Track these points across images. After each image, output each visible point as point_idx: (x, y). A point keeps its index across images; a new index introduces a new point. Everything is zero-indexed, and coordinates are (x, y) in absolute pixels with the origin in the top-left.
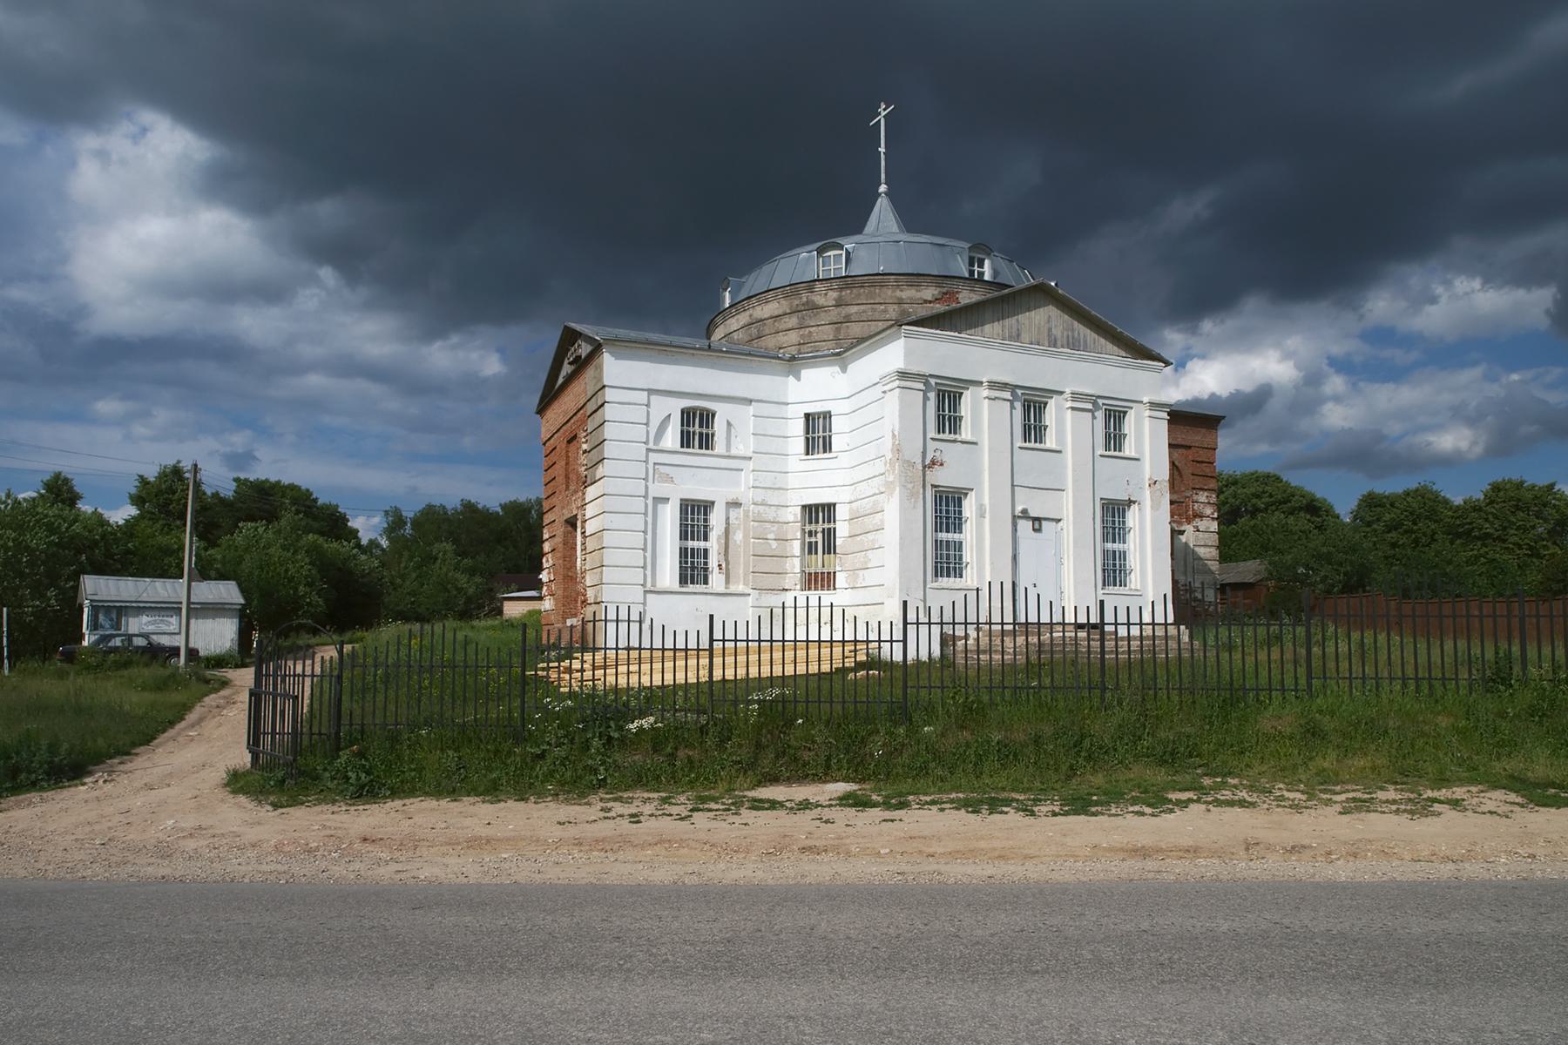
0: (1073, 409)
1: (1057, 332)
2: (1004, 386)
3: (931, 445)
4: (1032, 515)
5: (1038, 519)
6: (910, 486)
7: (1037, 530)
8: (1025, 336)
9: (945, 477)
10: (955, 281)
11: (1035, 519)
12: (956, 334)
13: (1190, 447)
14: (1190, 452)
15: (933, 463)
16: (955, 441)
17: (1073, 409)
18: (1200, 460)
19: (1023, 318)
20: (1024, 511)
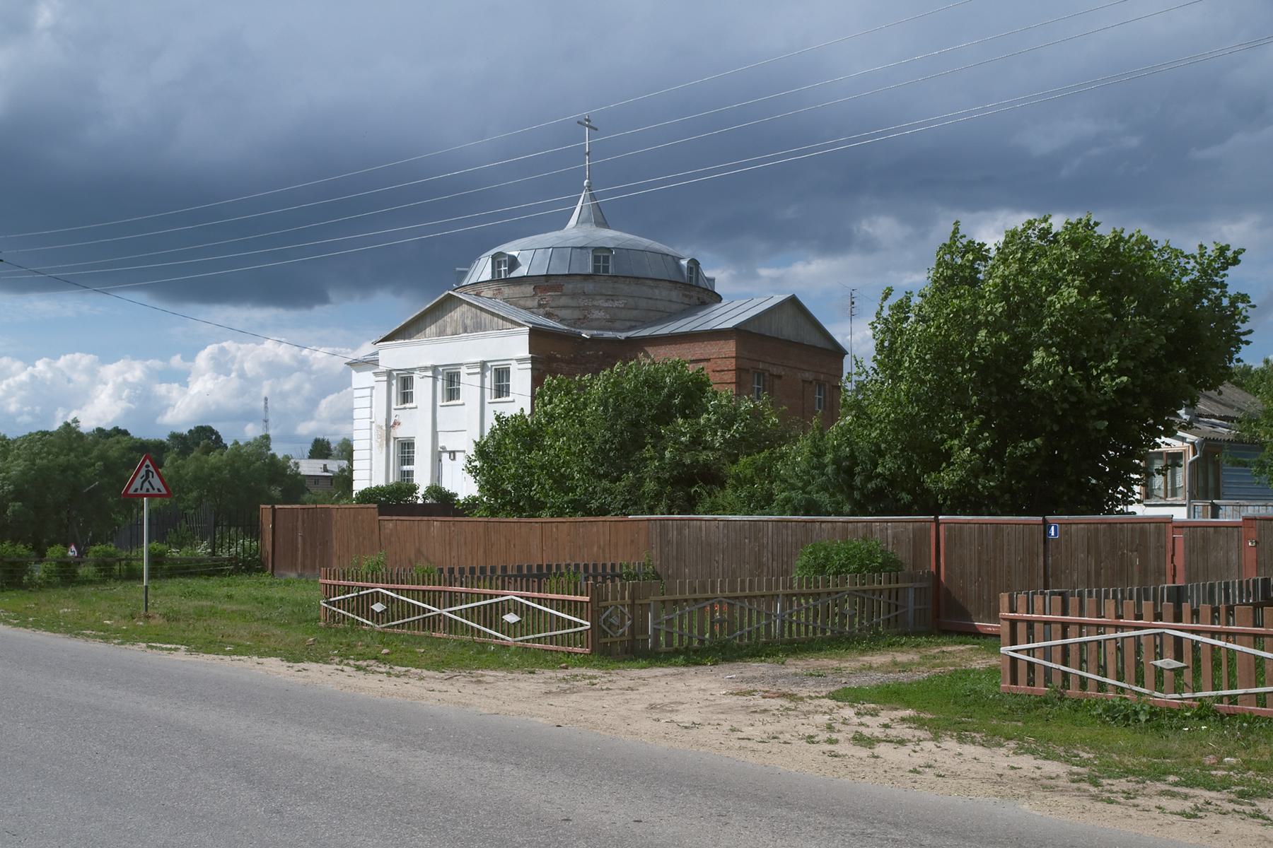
0: (469, 374)
1: (468, 322)
2: (426, 369)
3: (394, 413)
4: (448, 449)
5: (454, 452)
6: (379, 440)
7: (454, 459)
8: (449, 330)
9: (400, 432)
10: (479, 285)
11: (450, 452)
12: (402, 341)
13: (709, 360)
14: (710, 363)
15: (395, 423)
16: (405, 408)
17: (469, 374)
18: (718, 369)
19: (447, 318)
20: (443, 448)
